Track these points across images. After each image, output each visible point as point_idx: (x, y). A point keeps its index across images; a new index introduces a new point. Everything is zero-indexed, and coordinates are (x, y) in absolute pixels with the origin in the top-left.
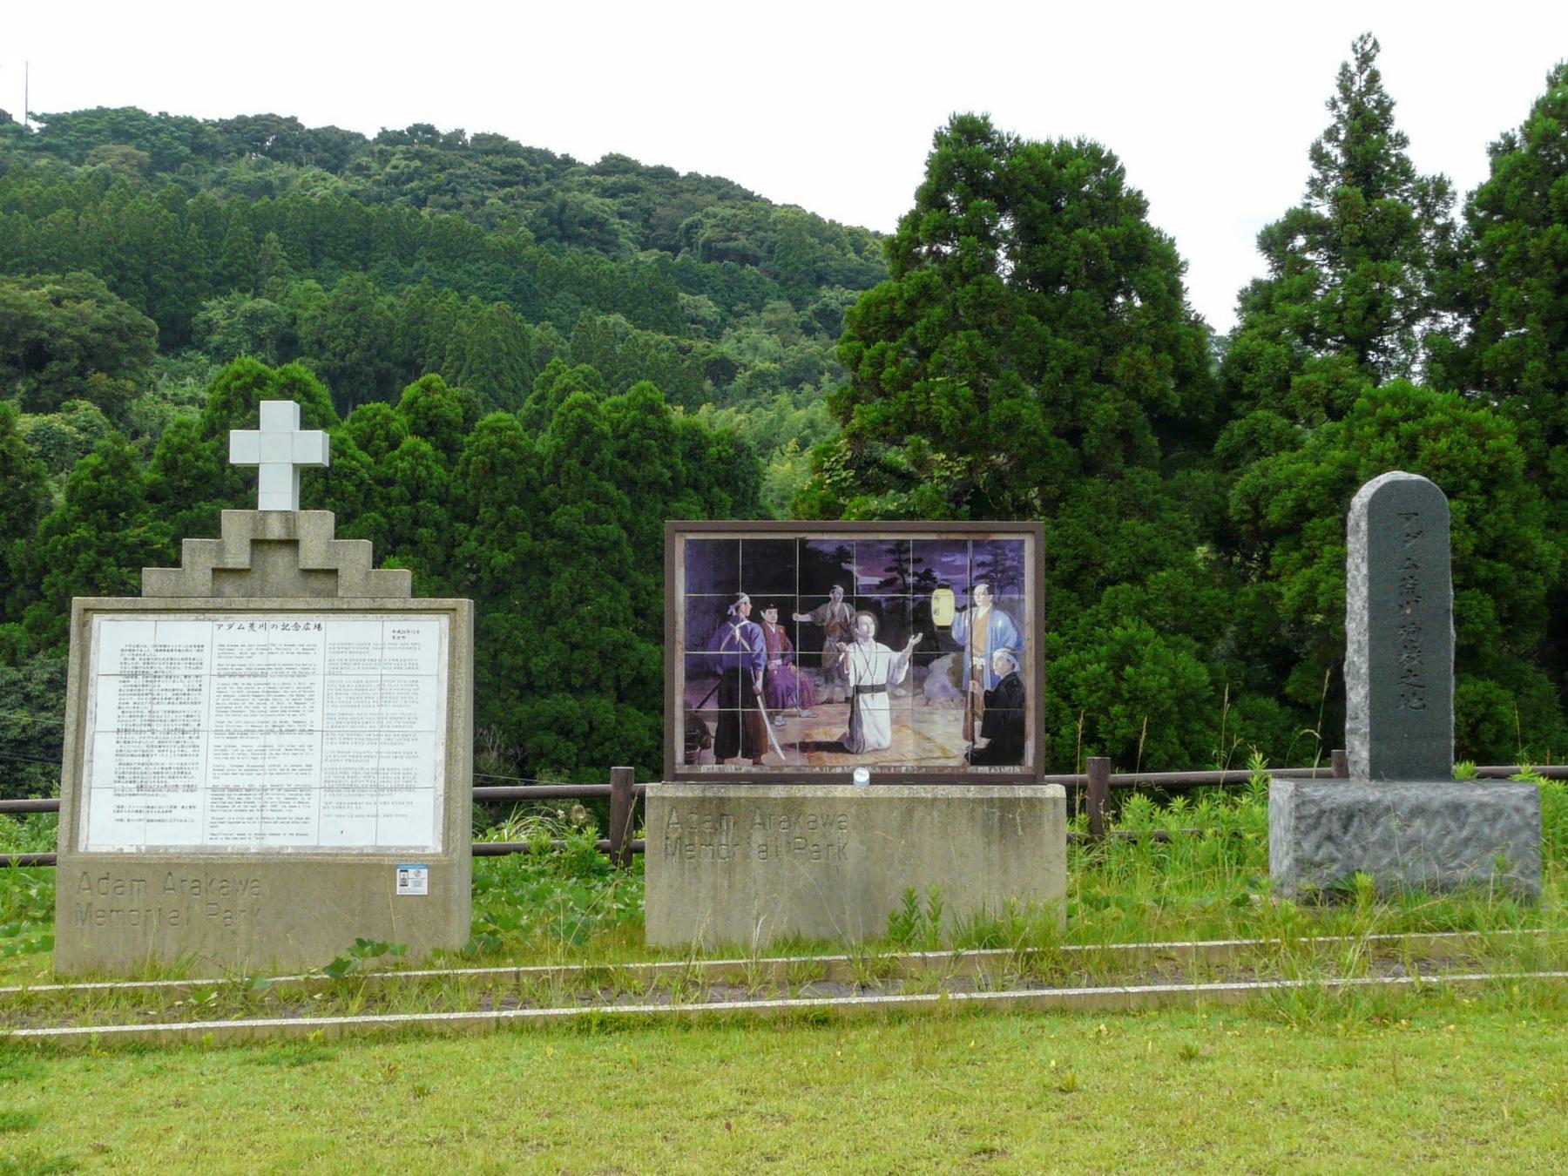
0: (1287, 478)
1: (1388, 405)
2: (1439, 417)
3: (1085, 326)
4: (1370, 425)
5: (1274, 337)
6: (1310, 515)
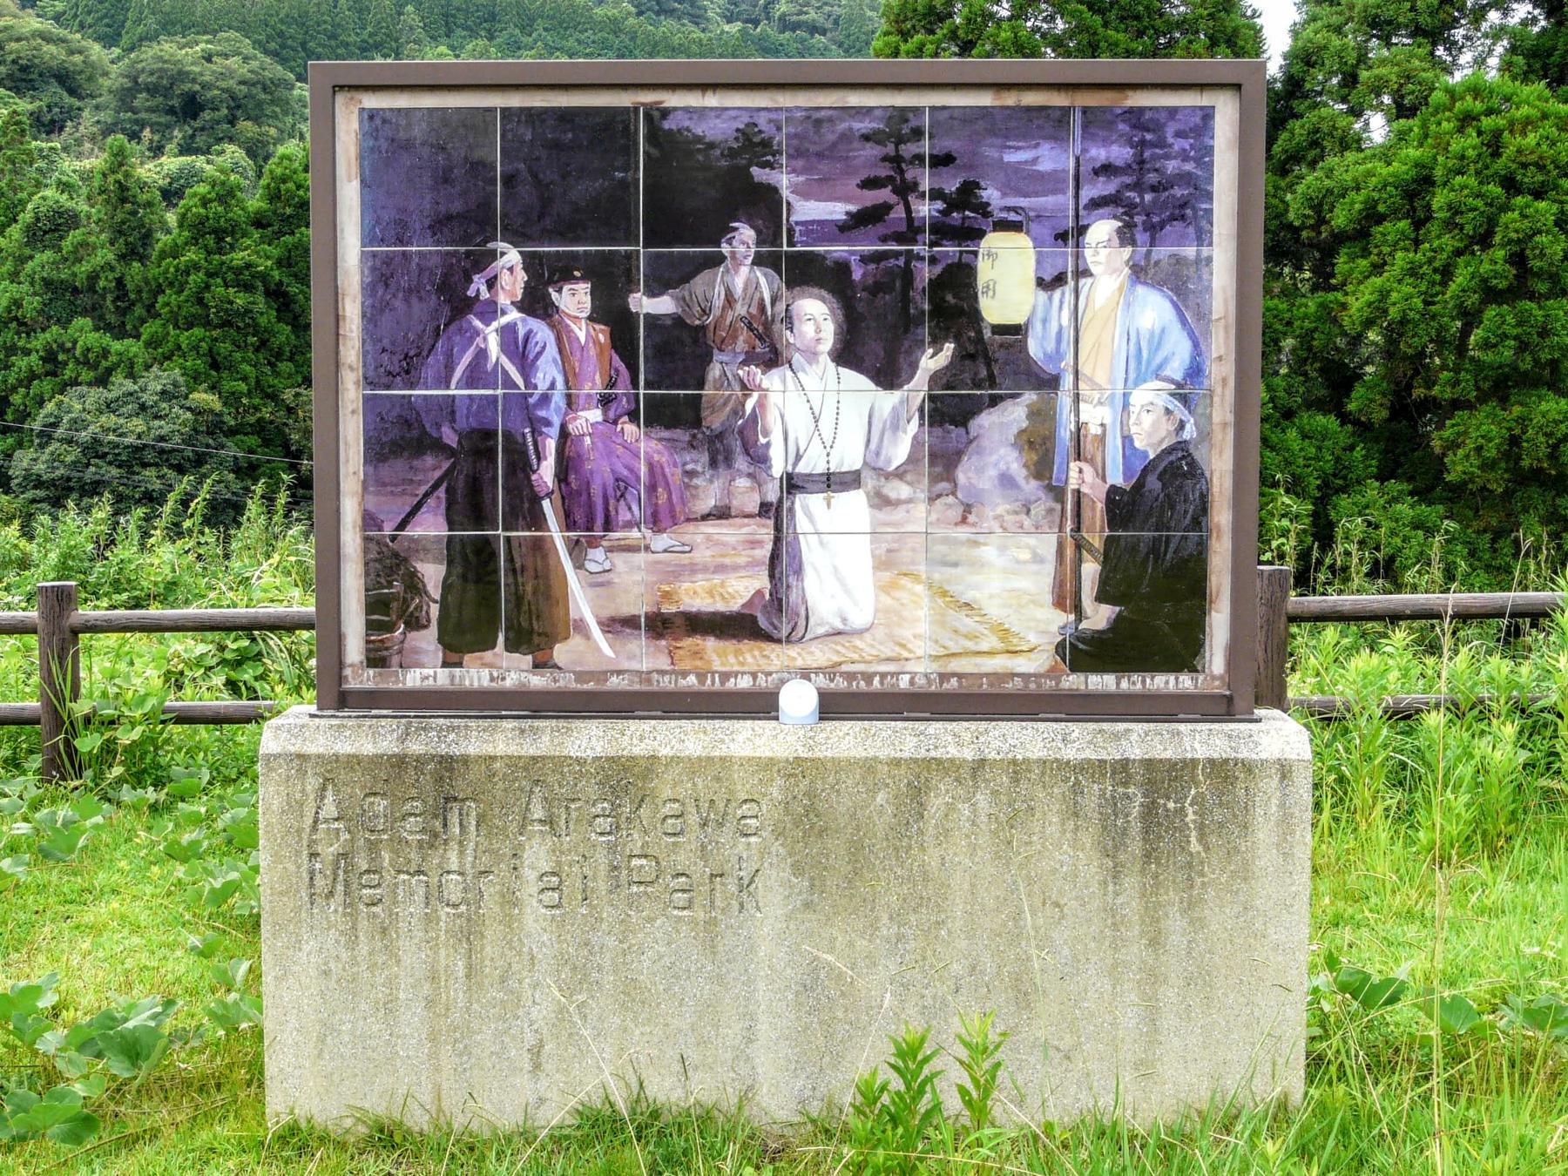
0: (1355, 180)
1: (1468, 98)
2: (1525, 110)
3: (1137, 18)
4: (1448, 120)
5: (1338, 30)
6: (1381, 219)
